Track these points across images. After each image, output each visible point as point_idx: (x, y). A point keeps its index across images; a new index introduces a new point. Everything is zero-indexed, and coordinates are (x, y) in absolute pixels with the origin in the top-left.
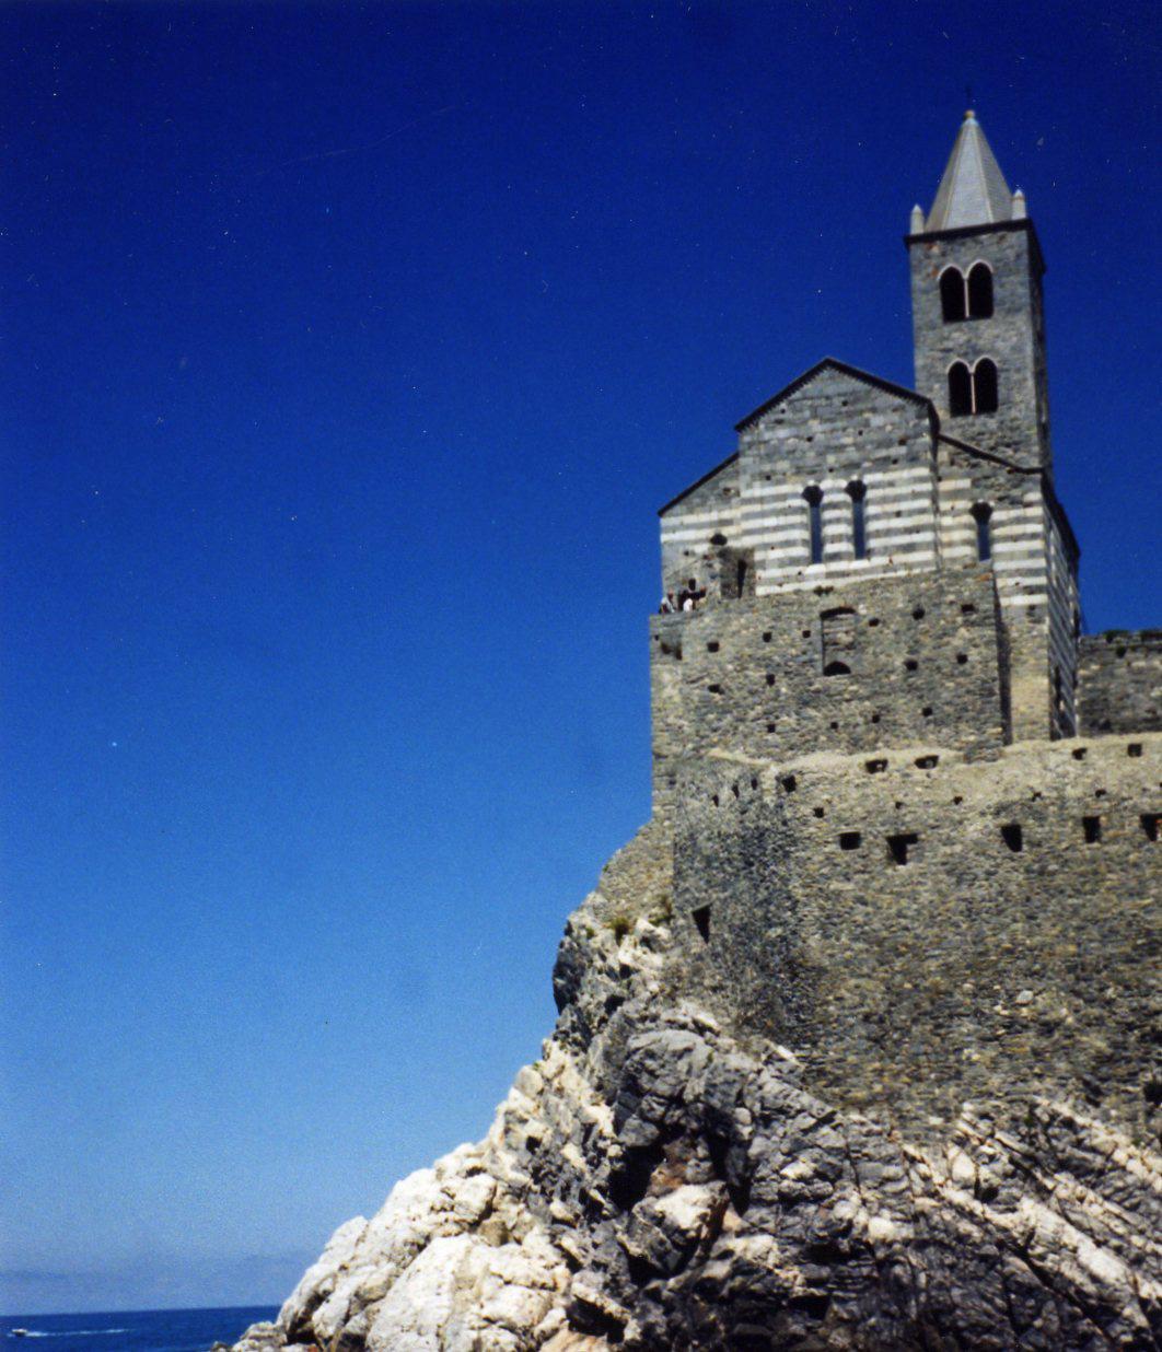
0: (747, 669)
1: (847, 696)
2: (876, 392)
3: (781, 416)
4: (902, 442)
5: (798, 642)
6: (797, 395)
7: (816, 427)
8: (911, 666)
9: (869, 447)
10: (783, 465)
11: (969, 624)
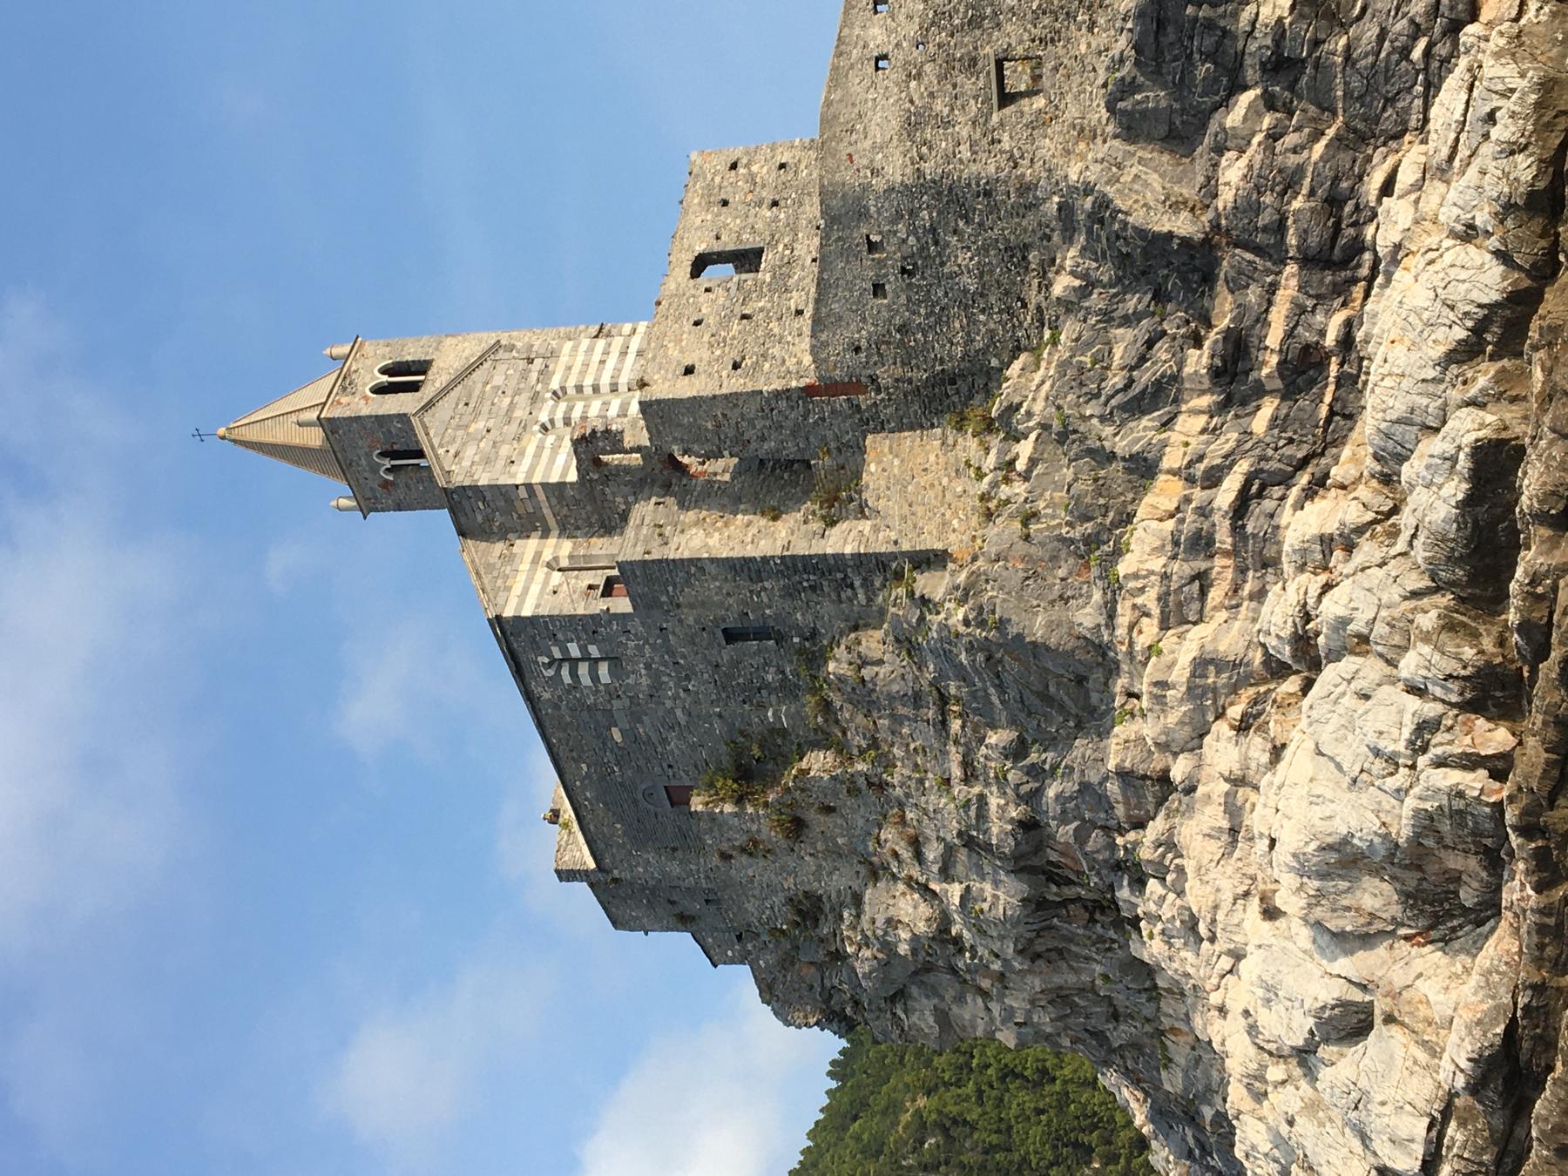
0: (725, 338)
1: (787, 252)
2: (469, 382)
3: (452, 452)
4: (531, 361)
5: (711, 295)
6: (436, 442)
7: (481, 425)
8: (775, 204)
9: (522, 386)
10: (505, 450)
11: (747, 166)
